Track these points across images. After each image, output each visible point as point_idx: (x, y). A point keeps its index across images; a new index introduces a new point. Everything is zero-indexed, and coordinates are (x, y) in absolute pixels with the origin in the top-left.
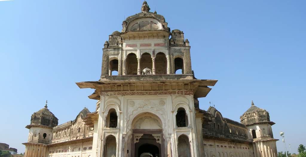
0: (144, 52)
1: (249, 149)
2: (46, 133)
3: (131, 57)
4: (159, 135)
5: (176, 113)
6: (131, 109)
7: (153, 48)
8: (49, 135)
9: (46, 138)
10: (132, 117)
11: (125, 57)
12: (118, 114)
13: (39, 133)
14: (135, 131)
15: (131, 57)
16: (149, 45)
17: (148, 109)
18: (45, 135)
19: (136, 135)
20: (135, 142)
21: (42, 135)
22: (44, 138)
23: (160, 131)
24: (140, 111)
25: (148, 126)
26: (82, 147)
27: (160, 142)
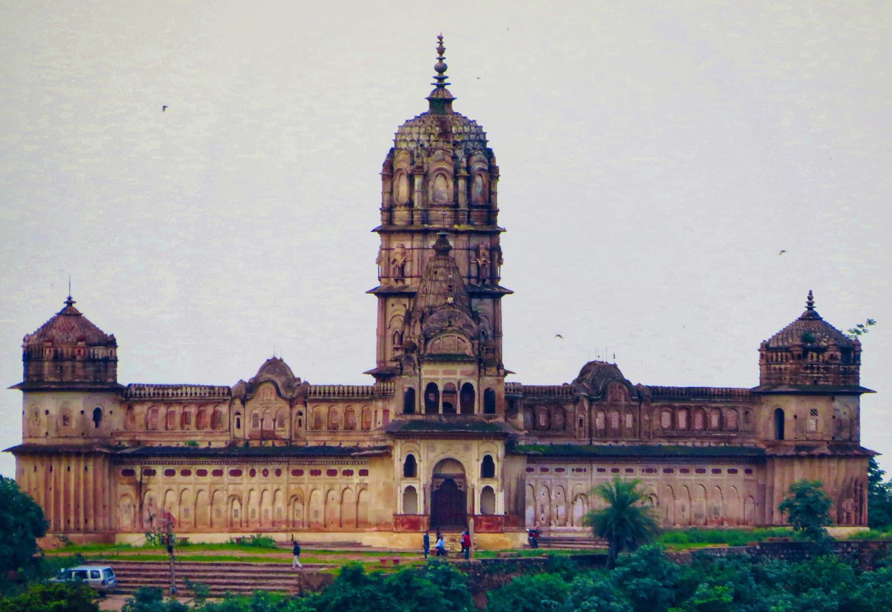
0: (448, 381)
1: (748, 472)
2: (101, 408)
3: (432, 387)
4: (461, 480)
5: (481, 461)
6: (432, 455)
7: (458, 376)
8: (111, 412)
9: (103, 424)
10: (433, 465)
11: (424, 388)
12: (417, 462)
13: (82, 412)
14: (435, 476)
15: (432, 387)
16: (454, 373)
17: (451, 455)
18: (98, 415)
19: (436, 480)
20: (435, 489)
21: (90, 414)
22: (97, 426)
23: (463, 476)
24: (442, 457)
25: (448, 471)
26: (288, 469)
27: (462, 489)
